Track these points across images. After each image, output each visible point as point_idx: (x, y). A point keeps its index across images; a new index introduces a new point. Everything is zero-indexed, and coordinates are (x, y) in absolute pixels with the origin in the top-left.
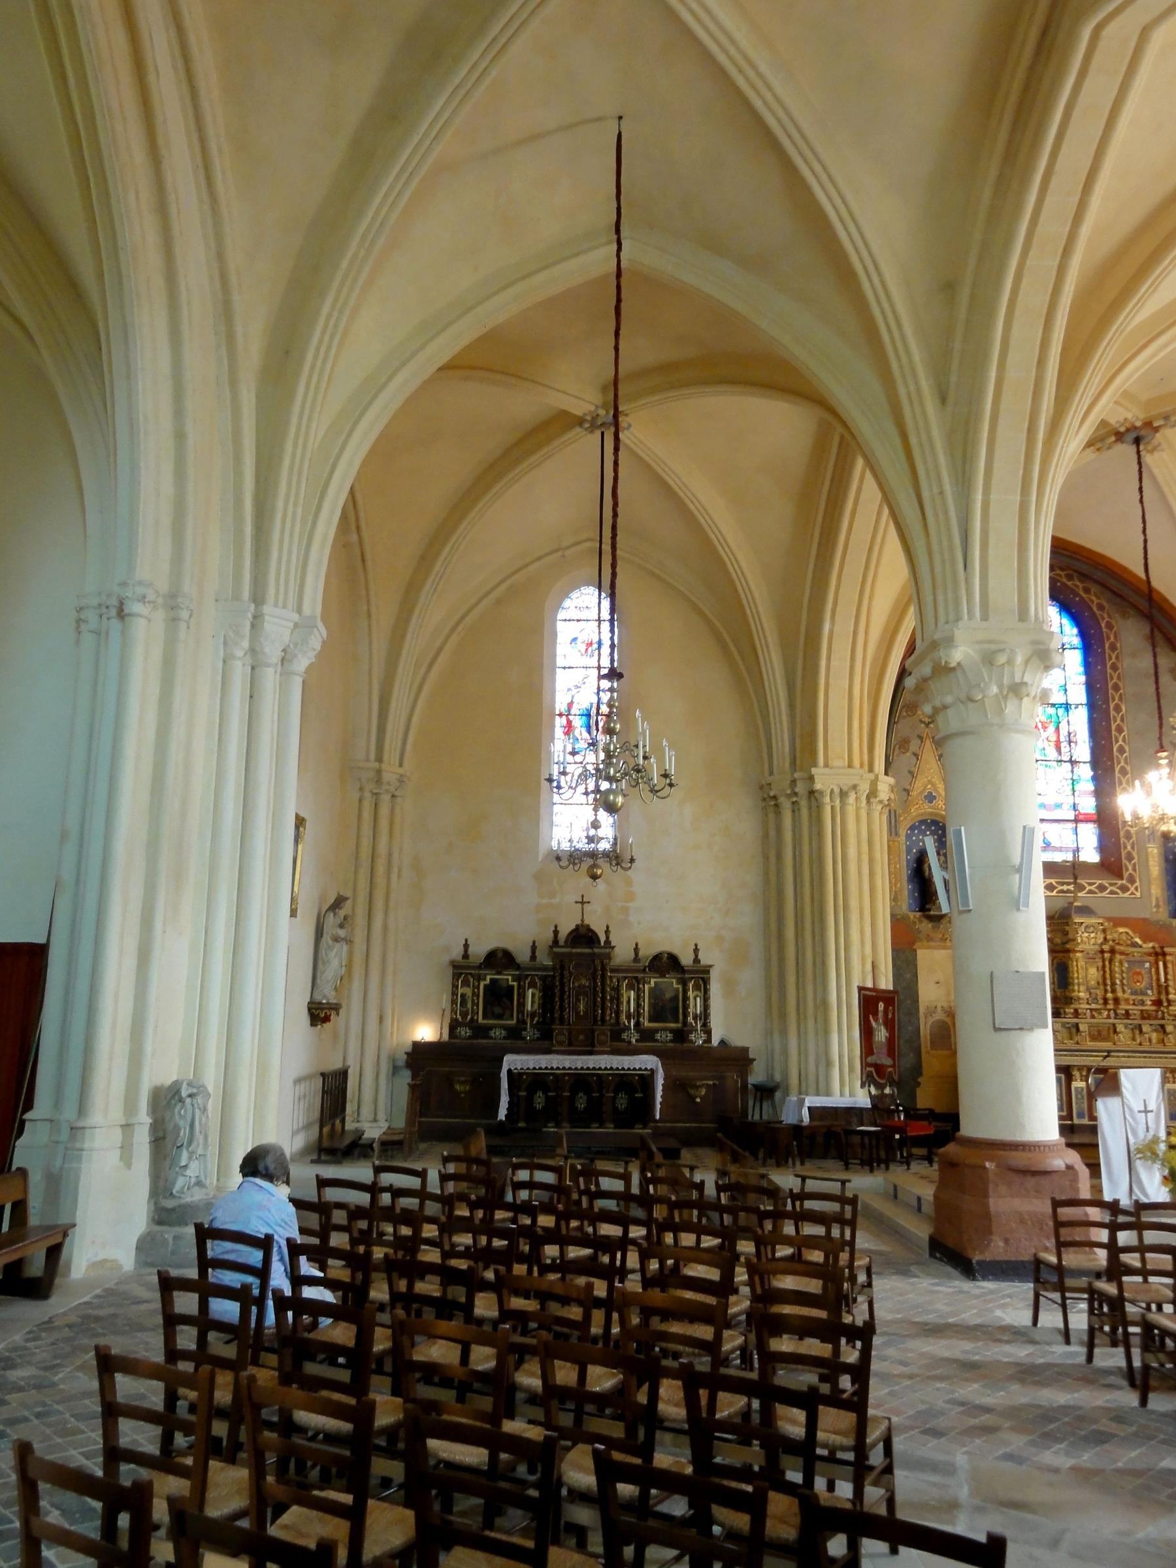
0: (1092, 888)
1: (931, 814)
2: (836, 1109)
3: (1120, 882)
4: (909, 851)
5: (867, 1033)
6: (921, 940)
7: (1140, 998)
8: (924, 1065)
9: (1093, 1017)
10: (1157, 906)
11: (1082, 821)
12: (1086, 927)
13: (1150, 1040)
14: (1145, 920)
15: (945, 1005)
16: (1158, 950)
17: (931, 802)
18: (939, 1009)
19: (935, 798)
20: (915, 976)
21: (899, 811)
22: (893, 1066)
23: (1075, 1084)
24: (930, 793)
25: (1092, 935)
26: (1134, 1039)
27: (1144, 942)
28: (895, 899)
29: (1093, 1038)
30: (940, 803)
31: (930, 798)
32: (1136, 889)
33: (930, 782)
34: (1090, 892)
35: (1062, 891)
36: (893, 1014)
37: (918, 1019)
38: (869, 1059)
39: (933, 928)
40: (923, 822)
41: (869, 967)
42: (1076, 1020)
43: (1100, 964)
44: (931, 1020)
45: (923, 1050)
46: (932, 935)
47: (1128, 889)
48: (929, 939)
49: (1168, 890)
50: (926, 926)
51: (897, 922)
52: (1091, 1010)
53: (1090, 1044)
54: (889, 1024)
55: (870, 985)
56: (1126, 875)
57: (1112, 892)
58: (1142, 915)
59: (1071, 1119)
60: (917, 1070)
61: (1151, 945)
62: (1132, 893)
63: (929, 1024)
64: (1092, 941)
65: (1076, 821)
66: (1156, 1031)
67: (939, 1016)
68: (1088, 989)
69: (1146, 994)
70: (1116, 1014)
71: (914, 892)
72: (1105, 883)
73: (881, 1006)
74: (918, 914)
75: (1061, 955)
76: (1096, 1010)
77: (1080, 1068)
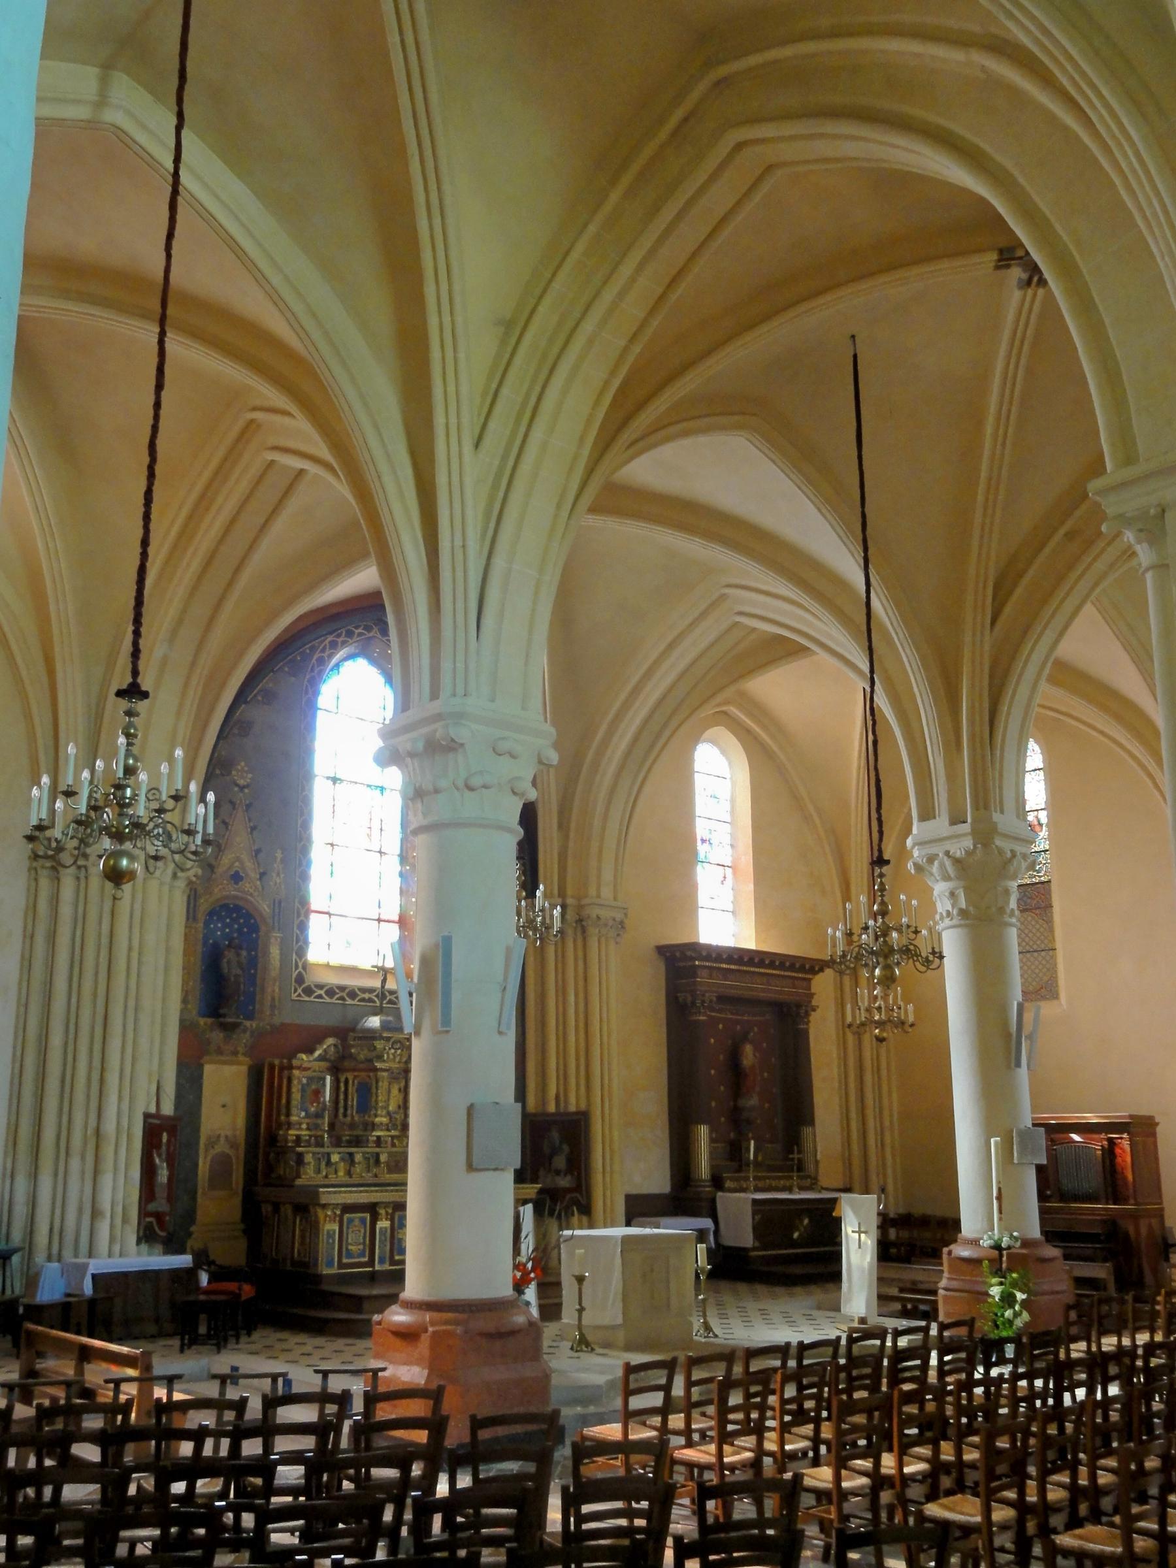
1: (236, 897)
2: (126, 1275)
4: (205, 943)
5: (148, 1171)
8: (199, 1212)
15: (229, 1133)
17: (236, 883)
18: (222, 1140)
19: (241, 879)
20: (199, 1097)
21: (200, 890)
24: (237, 873)
28: (185, 1001)
29: (390, 1171)
30: (246, 886)
31: (237, 878)
33: (238, 859)
35: (363, 1000)
40: (225, 907)
42: (378, 1150)
43: (403, 1084)
44: (212, 1152)
45: (200, 1191)
48: (219, 1052)
50: (217, 1036)
51: (186, 1028)
52: (393, 1137)
55: (153, 1110)
59: (371, 1262)
63: (209, 1158)
64: (397, 1059)
67: (222, 1147)
68: (389, 1114)
74: (210, 1020)
75: (363, 1074)
76: (397, 1137)
77: (386, 1205)
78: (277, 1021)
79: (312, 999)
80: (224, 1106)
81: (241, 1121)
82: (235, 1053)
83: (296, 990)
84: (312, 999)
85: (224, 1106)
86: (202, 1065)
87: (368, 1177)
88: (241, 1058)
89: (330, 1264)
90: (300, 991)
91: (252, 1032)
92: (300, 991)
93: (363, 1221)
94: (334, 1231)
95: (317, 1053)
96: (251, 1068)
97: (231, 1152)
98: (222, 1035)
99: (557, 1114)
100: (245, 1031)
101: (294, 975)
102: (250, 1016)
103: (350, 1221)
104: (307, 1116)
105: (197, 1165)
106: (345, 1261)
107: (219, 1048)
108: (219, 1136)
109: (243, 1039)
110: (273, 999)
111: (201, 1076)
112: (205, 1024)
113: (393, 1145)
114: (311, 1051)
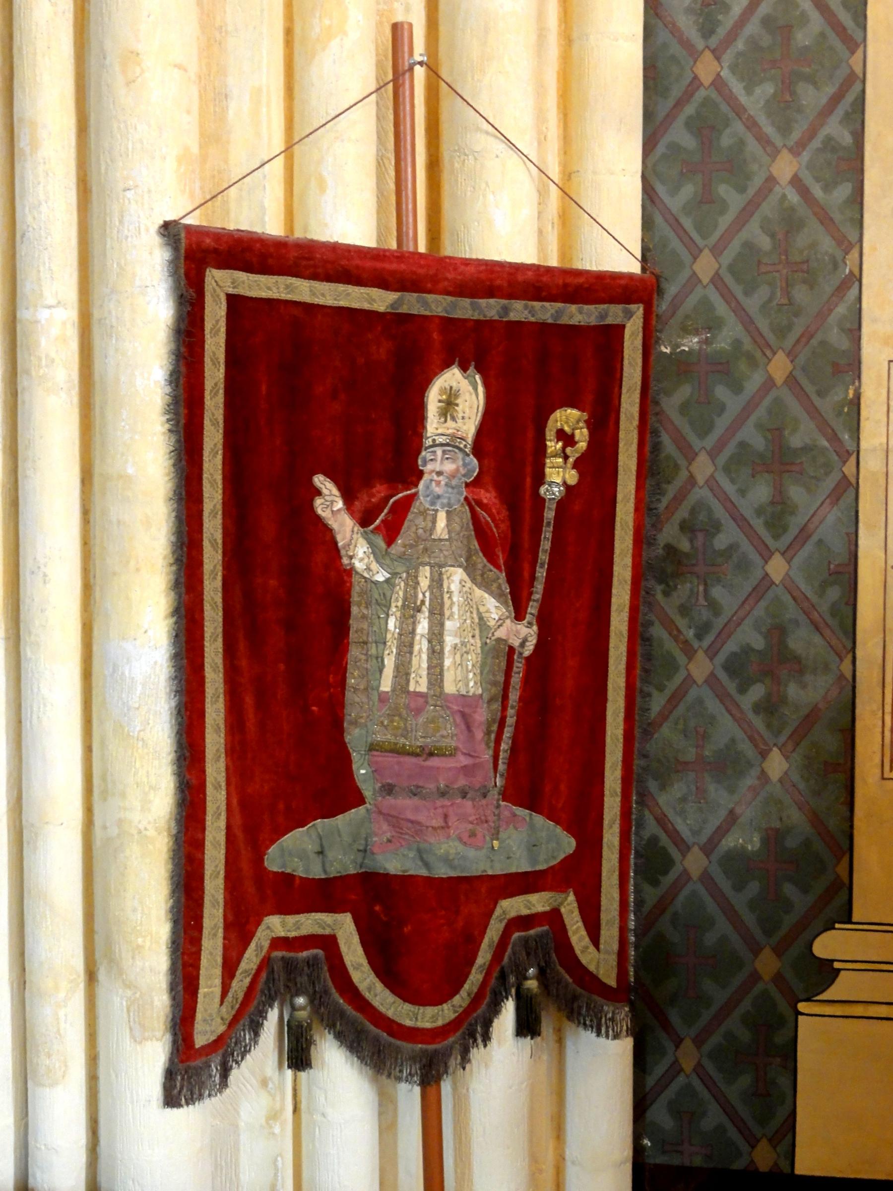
20: (850, 164)
22: (578, 874)
36: (598, 465)
38: (297, 851)
41: (347, 69)
54: (535, 544)
55: (349, 219)
73: (456, 404)
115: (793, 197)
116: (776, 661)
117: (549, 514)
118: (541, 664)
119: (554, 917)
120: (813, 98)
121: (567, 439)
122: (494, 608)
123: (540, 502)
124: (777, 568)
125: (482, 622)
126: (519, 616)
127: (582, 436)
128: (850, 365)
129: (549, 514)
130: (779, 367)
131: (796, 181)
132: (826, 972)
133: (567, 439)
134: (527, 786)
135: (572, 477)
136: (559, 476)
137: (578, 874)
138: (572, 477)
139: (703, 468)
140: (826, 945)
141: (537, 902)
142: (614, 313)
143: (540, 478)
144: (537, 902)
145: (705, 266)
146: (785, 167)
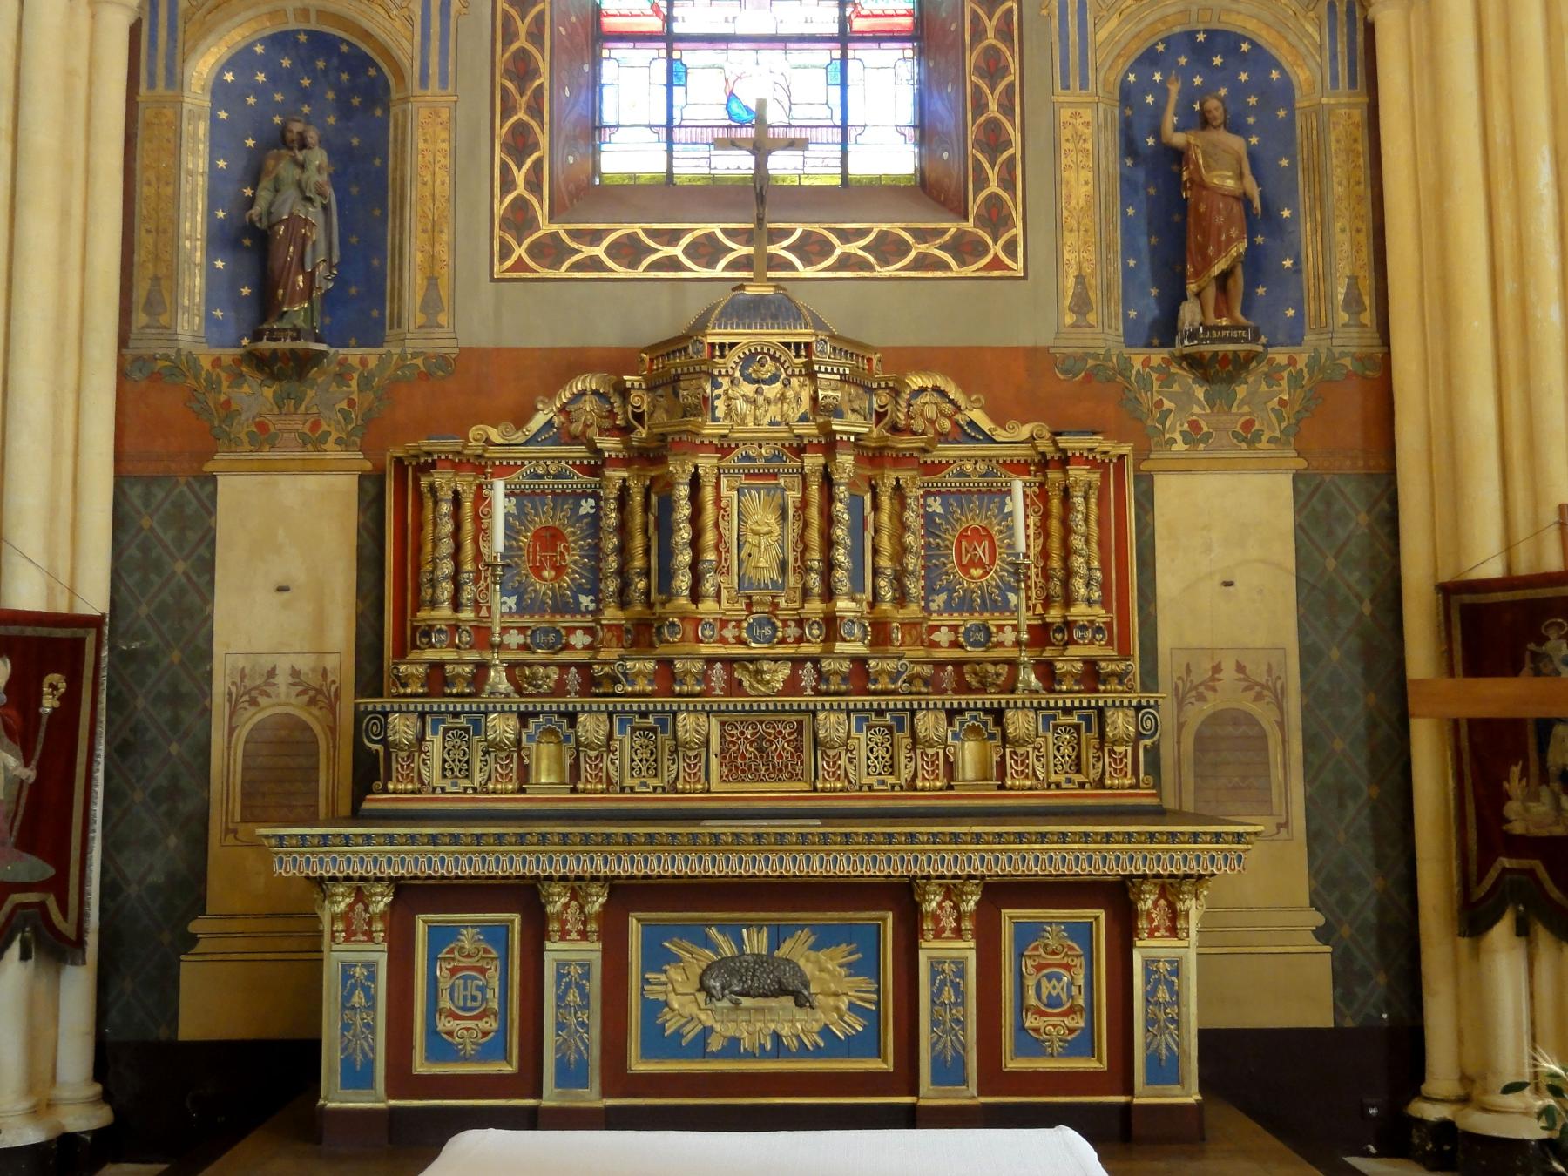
0: (854, 248)
3: (953, 228)
6: (234, 444)
7: (976, 619)
9: (734, 687)
10: (1081, 304)
11: (862, 38)
12: (749, 359)
13: (950, 767)
14: (1035, 356)
15: (304, 664)
16: (1045, 446)
18: (282, 679)
20: (208, 566)
23: (555, 952)
25: (772, 391)
26: (892, 768)
27: (999, 419)
32: (1010, 249)
34: (846, 262)
36: (71, 700)
37: (207, 712)
39: (279, 400)
43: (793, 495)
44: (250, 719)
46: (275, 424)
47: (979, 249)
48: (263, 436)
49: (1129, 249)
50: (255, 397)
51: (142, 375)
52: (729, 661)
53: (721, 788)
56: (973, 208)
57: (923, 262)
58: (1025, 338)
60: (189, 890)
61: (1025, 431)
62: (996, 263)
63: (243, 732)
65: (844, 38)
66: (974, 730)
67: (283, 701)
69: (1004, 607)
70: (821, 676)
71: (234, 288)
72: (896, 228)
77: (576, 886)
78: (443, 343)
79: (562, 272)
80: (282, 589)
81: (340, 634)
82: (313, 439)
83: (506, 252)
84: (562, 272)
85: (282, 589)
86: (212, 479)
87: (645, 791)
88: (332, 453)
89: (357, 1077)
90: (520, 251)
91: (365, 383)
92: (520, 251)
93: (496, 936)
94: (371, 967)
95: (539, 421)
96: (363, 478)
97: (313, 719)
98: (268, 392)
99: (1508, 582)
100: (342, 377)
101: (500, 208)
102: (372, 334)
103: (441, 938)
104: (522, 609)
105: (204, 750)
106: (421, 1066)
107: (262, 427)
108: (272, 673)
109: (326, 398)
110: (432, 281)
111: (209, 506)
112: (217, 362)
113: (734, 687)
114: (520, 422)
115: (184, 580)
116: (173, 792)
117: (44, 721)
118: (36, 789)
119: (42, 905)
120: (192, 536)
121: (54, 687)
122: (12, 762)
123: (39, 716)
124: (174, 748)
125: (6, 768)
126: (27, 765)
127: (63, 687)
128: (208, 655)
129: (44, 721)
130: (176, 656)
131: (185, 574)
132: (193, 940)
133: (54, 687)
134: (29, 840)
135: (57, 704)
136: (49, 704)
137: (58, 885)
138: (57, 704)
139: (140, 702)
140: (193, 927)
141: (32, 897)
142: (80, 632)
143: (39, 704)
144: (32, 897)
145: (144, 610)
146: (180, 567)
